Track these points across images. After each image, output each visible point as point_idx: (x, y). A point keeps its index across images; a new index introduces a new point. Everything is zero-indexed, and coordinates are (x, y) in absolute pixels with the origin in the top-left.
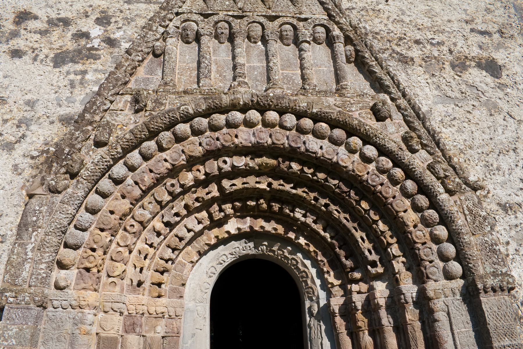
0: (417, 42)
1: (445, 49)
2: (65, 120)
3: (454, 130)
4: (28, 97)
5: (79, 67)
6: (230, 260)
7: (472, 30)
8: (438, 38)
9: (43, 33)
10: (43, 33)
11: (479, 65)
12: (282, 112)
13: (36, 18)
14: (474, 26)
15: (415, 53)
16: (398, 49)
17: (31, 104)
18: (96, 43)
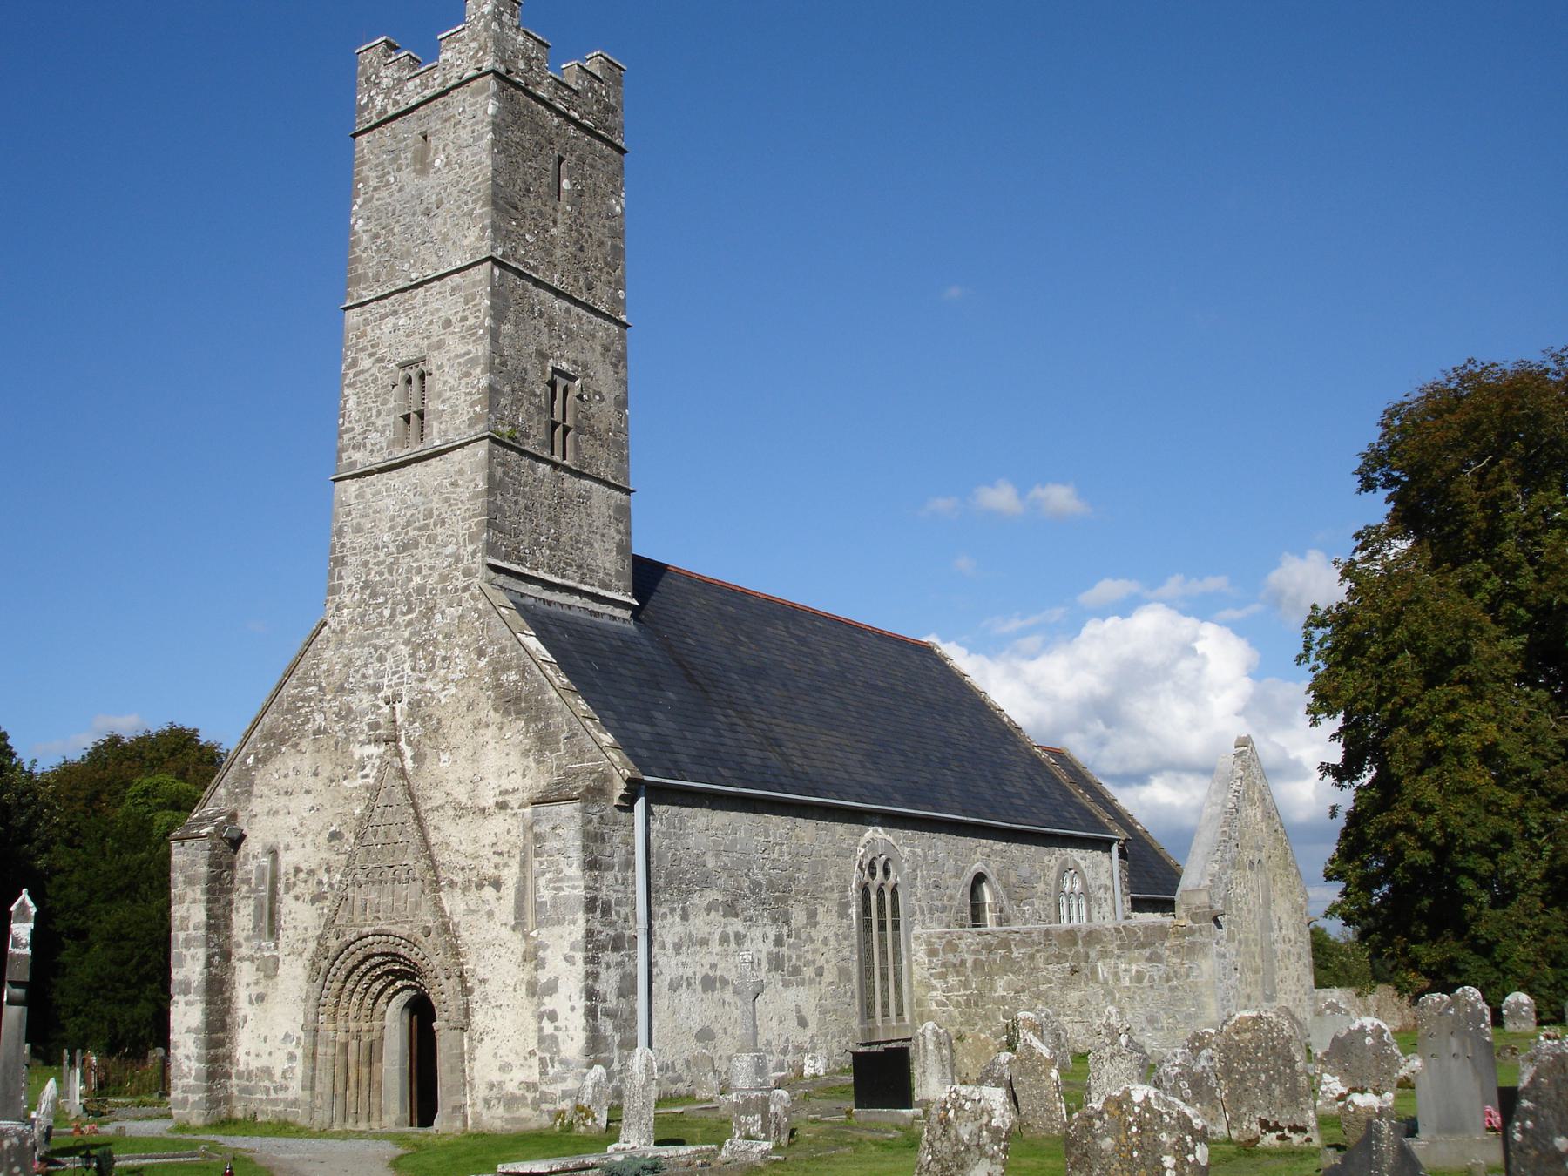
0: (463, 869)
1: (475, 872)
3: (468, 933)
4: (305, 925)
5: (321, 905)
6: (408, 998)
7: (494, 853)
8: (474, 863)
10: (305, 882)
11: (489, 884)
12: (388, 936)
13: (302, 871)
14: (495, 849)
15: (459, 878)
16: (452, 877)
18: (325, 888)
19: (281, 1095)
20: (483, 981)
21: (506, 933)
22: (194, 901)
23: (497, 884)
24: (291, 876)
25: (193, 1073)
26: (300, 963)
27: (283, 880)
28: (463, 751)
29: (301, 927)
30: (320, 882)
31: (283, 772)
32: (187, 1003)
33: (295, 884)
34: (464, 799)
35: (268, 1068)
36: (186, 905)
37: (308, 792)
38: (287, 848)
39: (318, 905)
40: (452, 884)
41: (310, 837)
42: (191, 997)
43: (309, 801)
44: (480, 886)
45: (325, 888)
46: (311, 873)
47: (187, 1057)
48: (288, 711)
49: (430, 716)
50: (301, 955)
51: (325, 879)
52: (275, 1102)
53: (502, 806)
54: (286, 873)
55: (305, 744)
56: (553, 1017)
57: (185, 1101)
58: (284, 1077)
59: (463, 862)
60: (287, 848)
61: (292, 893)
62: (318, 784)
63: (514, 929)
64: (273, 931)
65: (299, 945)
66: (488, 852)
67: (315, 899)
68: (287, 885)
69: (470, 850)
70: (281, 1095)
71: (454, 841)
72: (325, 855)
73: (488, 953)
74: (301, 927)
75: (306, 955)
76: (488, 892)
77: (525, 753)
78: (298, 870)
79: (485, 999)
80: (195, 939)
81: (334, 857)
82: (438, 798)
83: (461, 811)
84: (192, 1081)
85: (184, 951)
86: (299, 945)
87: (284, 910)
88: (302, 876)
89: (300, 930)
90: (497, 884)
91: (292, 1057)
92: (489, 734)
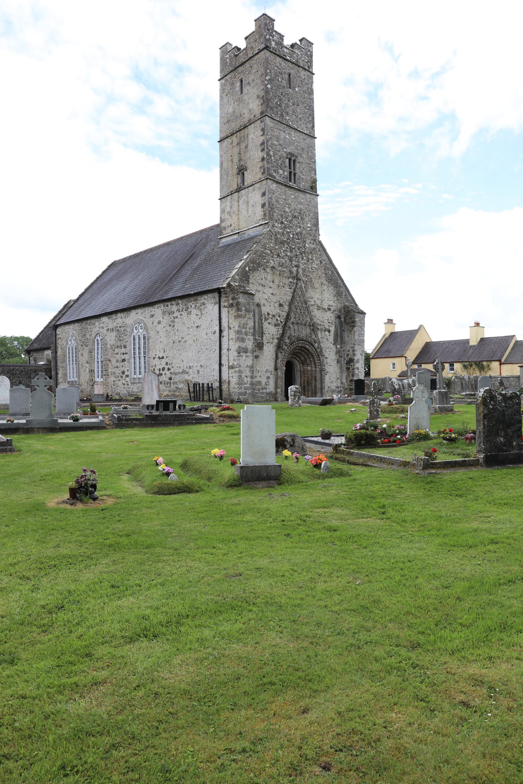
2: (278, 338)
9: (272, 318)
15: (319, 328)
17: (273, 335)
18: (279, 322)
19: (264, 391)
20: (326, 358)
21: (332, 345)
22: (250, 318)
23: (329, 331)
24: (266, 315)
25: (249, 382)
26: (272, 345)
27: (263, 316)
28: (319, 290)
29: (271, 334)
30: (277, 320)
31: (260, 277)
32: (246, 356)
33: (268, 319)
34: (319, 304)
35: (260, 381)
36: (246, 319)
37: (270, 287)
38: (264, 305)
39: (277, 327)
40: (318, 329)
41: (272, 304)
42: (249, 354)
43: (271, 291)
44: (325, 331)
45: (279, 322)
46: (274, 316)
47: (247, 377)
48: (260, 256)
49: (309, 276)
50: (272, 343)
51: (279, 319)
52: (262, 393)
53: (329, 309)
54: (264, 314)
55: (268, 270)
56: (358, 369)
57: (246, 392)
58: (266, 385)
59: (320, 323)
60: (264, 305)
61: (267, 322)
62: (274, 286)
63: (334, 344)
64: (262, 334)
65: (272, 341)
66: (326, 321)
67: (275, 326)
68: (265, 318)
69: (322, 320)
70: (264, 391)
71: (317, 316)
72: (278, 311)
73: (327, 350)
74: (271, 334)
75: (274, 344)
76: (327, 333)
77: (334, 296)
78: (268, 314)
79: (327, 363)
80: (249, 332)
81: (281, 312)
82: (312, 303)
83: (319, 308)
84: (248, 385)
85: (245, 337)
86: (272, 341)
87: (264, 327)
88: (270, 316)
89: (271, 335)
90: (329, 331)
91: (268, 378)
92: (325, 287)
